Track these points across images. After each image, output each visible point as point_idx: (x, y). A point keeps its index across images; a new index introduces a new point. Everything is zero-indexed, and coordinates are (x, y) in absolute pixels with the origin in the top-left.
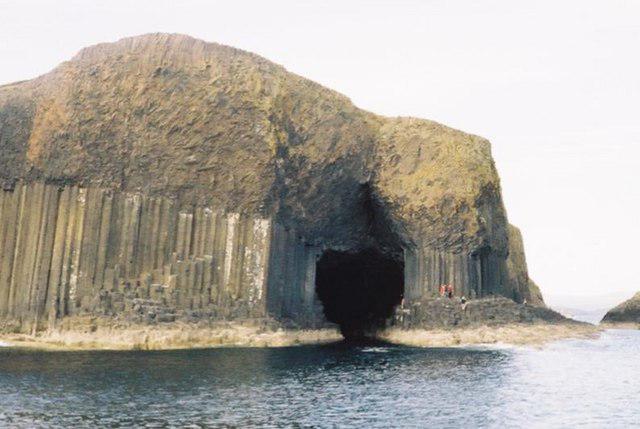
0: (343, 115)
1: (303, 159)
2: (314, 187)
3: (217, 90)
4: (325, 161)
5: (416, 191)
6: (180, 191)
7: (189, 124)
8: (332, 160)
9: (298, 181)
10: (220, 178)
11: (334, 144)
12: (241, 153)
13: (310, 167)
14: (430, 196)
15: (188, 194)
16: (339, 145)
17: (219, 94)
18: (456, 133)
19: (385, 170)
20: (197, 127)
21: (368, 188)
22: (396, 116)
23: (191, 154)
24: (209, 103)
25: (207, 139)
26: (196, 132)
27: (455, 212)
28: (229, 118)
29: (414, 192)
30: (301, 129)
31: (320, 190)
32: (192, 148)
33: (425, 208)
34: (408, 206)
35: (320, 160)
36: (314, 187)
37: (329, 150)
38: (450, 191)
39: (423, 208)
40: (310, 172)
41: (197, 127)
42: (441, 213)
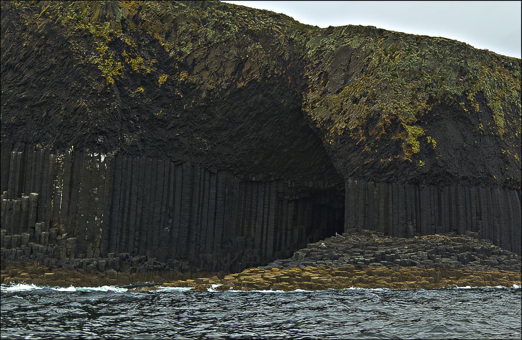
0: (251, 33)
1: (188, 88)
3: (46, 22)
4: (229, 87)
5: (341, 111)
7: (21, 61)
8: (241, 85)
10: (52, 112)
11: (240, 65)
14: (355, 116)
16: (247, 67)
17: (48, 25)
19: (313, 91)
20: (29, 61)
23: (23, 91)
24: (39, 36)
25: (38, 74)
26: (30, 67)
27: (383, 132)
28: (60, 49)
29: (338, 112)
30: (181, 54)
32: (24, 84)
33: (349, 131)
35: (218, 87)
37: (233, 74)
38: (376, 107)
39: (346, 131)
40: (206, 100)
42: (366, 134)
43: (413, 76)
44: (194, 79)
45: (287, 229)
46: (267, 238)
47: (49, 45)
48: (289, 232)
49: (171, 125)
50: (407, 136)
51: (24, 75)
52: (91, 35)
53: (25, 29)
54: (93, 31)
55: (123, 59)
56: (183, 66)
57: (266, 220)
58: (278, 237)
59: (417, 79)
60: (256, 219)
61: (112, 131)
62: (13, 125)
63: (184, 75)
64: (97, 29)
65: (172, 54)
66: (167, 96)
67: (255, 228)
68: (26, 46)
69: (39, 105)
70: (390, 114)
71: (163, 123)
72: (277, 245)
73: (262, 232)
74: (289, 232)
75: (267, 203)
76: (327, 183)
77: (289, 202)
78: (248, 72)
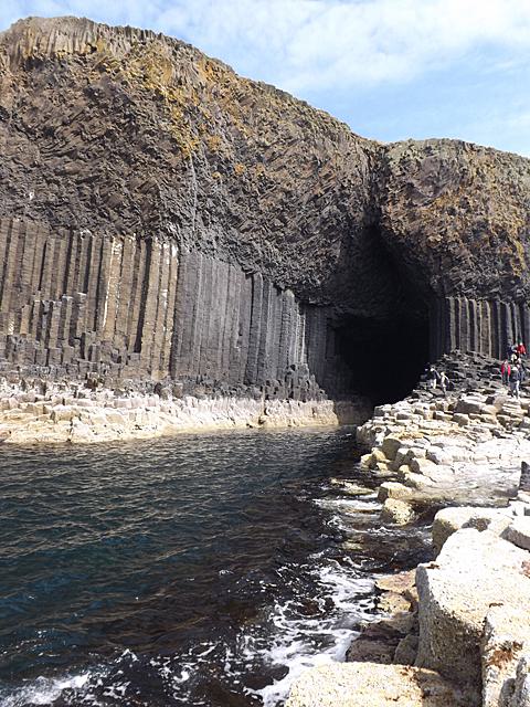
1: (266, 183)
2: (293, 223)
6: (47, 209)
8: (319, 191)
9: (261, 213)
12: (139, 154)
13: (280, 196)
15: (62, 213)
16: (325, 171)
18: (490, 151)
20: (75, 126)
21: (375, 227)
22: (405, 139)
31: (305, 231)
32: (68, 154)
34: (423, 245)
36: (293, 223)
41: (75, 126)
43: (512, 190)
44: (271, 176)
47: (105, 106)
49: (245, 226)
50: (514, 250)
51: (67, 143)
52: (162, 97)
53: (72, 85)
54: (164, 91)
55: (200, 132)
56: (260, 159)
59: (515, 193)
61: (187, 219)
62: (48, 204)
63: (262, 167)
64: (171, 93)
65: (250, 142)
66: (244, 190)
68: (72, 106)
69: (88, 181)
70: (497, 226)
71: (236, 220)
78: (326, 176)
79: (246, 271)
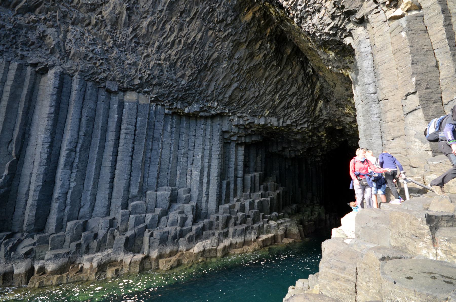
45: (236, 177)
46: (208, 188)
48: (239, 180)
57: (206, 165)
58: (224, 186)
60: (192, 164)
67: (191, 175)
72: (224, 196)
73: (201, 181)
74: (239, 180)
75: (208, 144)
76: (281, 121)
77: (238, 145)
79: (34, 65)
